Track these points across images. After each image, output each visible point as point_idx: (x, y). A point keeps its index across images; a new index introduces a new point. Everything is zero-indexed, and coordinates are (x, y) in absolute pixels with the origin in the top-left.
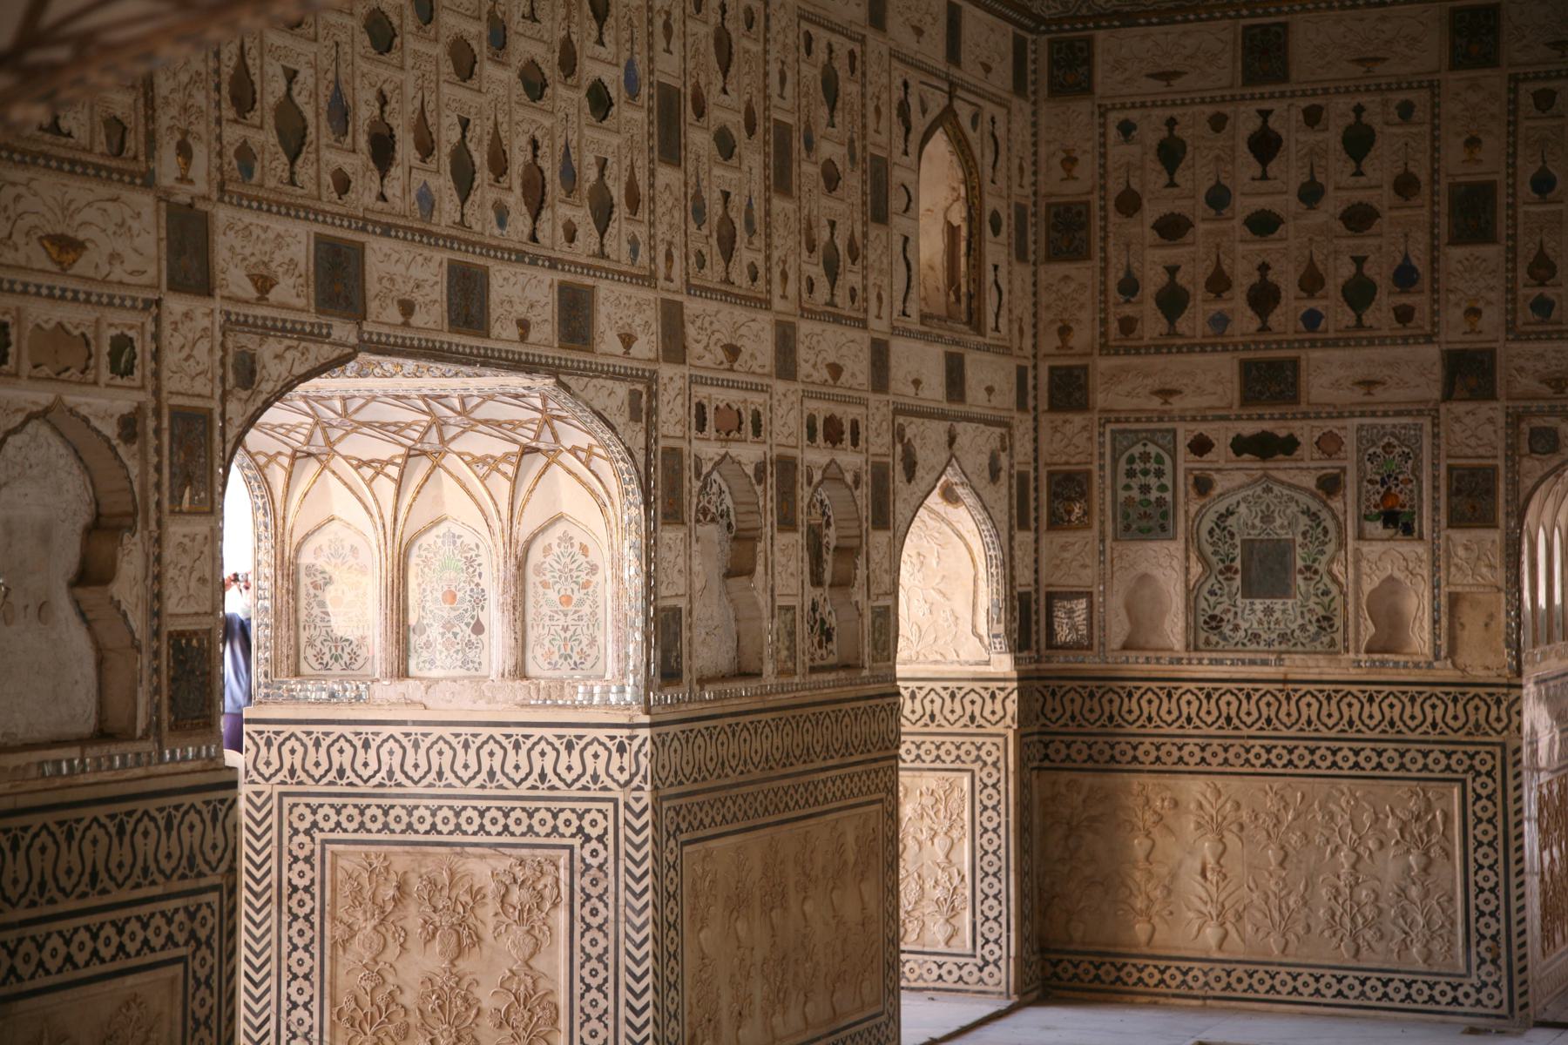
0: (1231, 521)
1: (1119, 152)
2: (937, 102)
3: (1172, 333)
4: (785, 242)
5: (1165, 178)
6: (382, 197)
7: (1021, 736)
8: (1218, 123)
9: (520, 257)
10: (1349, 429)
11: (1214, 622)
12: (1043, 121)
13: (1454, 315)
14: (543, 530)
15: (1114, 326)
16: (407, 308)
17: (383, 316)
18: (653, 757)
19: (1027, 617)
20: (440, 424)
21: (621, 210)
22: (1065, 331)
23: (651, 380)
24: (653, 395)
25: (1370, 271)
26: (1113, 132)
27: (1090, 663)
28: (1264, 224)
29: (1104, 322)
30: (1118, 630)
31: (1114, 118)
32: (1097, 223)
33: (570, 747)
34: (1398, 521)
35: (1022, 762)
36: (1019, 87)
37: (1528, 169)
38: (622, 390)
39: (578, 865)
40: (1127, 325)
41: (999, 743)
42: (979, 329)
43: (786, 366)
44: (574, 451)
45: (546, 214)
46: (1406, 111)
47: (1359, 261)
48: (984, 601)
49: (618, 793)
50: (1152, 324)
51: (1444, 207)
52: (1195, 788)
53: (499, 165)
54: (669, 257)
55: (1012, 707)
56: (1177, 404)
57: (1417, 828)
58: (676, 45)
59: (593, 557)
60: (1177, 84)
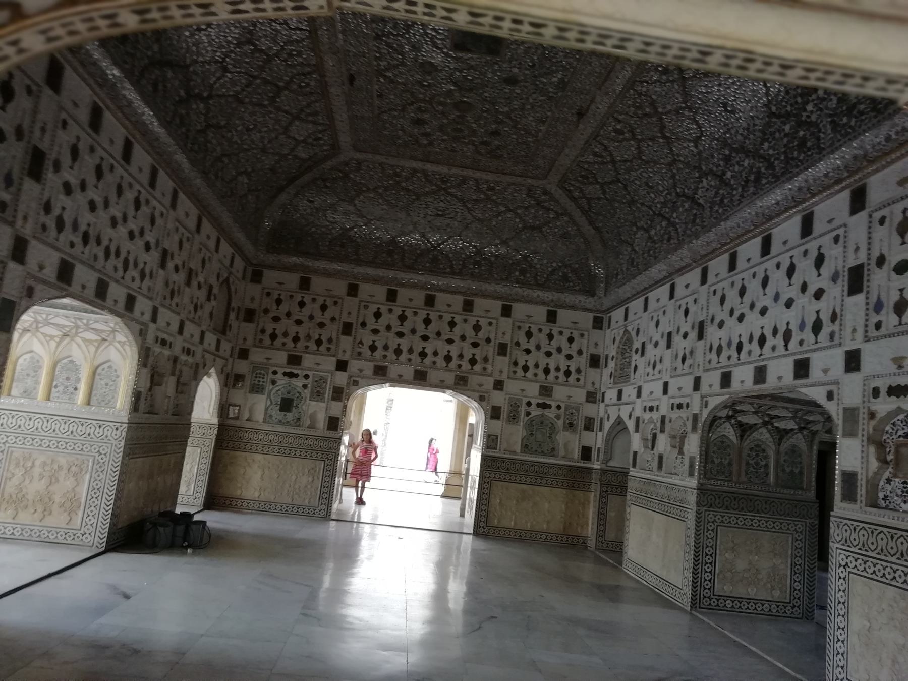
4: (186, 300)
6: (83, 253)
8: (291, 296)
9: (117, 282)
13: (340, 351)
16: (84, 287)
19: (223, 409)
20: (77, 327)
22: (245, 339)
25: (322, 338)
27: (238, 423)
30: (246, 416)
36: (244, 278)
37: (361, 320)
39: (96, 462)
40: (261, 341)
43: (181, 331)
44: (119, 342)
45: (127, 272)
46: (336, 303)
47: (320, 335)
49: (114, 443)
50: (267, 341)
51: (341, 326)
52: (259, 457)
53: (118, 254)
56: (271, 361)
57: (312, 471)
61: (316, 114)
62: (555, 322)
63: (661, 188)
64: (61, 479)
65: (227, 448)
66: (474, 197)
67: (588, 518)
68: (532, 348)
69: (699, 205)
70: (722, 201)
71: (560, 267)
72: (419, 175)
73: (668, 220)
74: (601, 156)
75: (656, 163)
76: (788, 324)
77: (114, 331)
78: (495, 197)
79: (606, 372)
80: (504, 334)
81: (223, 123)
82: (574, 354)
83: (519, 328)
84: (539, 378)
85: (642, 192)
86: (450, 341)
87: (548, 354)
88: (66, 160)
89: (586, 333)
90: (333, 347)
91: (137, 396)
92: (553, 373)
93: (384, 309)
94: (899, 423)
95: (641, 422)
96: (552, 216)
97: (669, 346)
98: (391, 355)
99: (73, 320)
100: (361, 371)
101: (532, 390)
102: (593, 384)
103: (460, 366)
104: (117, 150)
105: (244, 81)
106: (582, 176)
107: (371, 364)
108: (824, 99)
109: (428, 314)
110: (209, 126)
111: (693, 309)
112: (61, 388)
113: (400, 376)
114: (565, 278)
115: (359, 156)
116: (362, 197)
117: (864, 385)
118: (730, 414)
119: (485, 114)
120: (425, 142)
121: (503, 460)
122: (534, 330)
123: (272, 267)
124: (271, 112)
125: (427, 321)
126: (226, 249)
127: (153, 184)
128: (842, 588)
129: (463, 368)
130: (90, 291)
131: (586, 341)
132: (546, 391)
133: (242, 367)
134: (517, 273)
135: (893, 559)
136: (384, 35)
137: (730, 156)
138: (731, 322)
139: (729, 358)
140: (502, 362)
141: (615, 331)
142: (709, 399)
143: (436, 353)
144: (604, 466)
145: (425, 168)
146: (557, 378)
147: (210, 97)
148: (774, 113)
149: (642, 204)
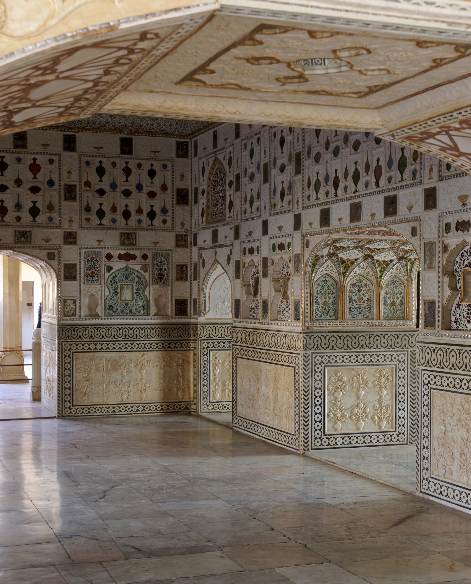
5: (99, 179)
62: (130, 152)
67: (189, 381)
68: (107, 188)
76: (378, 160)
79: (197, 210)
80: (69, 172)
83: (88, 163)
84: (117, 224)
89: (169, 164)
92: (134, 217)
94: (465, 254)
95: (241, 266)
97: (266, 180)
102: (183, 224)
103: (19, 219)
117: (439, 221)
121: (85, 327)
122: (106, 165)
128: (426, 403)
129: (23, 221)
131: (170, 174)
135: (460, 371)
138: (327, 156)
139: (327, 194)
140: (71, 210)
141: (204, 159)
142: (310, 238)
146: (140, 221)
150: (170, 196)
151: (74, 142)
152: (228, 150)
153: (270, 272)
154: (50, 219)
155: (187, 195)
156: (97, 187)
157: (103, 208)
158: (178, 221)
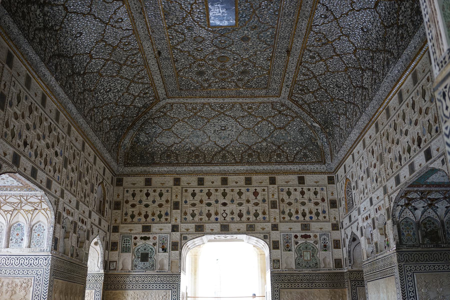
0: (140, 250)
1: (126, 194)
2: (101, 180)
3: (132, 221)
4: (79, 189)
7: (104, 283)
8: (141, 191)
10: (157, 236)
11: (136, 266)
12: (115, 189)
14: (36, 223)
15: (123, 220)
17: (21, 169)
18: (51, 261)
19: (107, 264)
20: (21, 202)
21: (57, 171)
22: (116, 220)
23: (58, 199)
24: (58, 202)
25: (162, 213)
26: (125, 191)
27: (116, 272)
28: (147, 206)
29: (122, 219)
30: (121, 267)
31: (126, 189)
32: (122, 205)
33: (36, 259)
34: (164, 250)
35: (104, 288)
36: (112, 183)
37: (184, 200)
38: (54, 199)
39: (36, 279)
40: (125, 220)
41: (100, 285)
42: (104, 216)
43: (77, 208)
44: (44, 209)
45: (47, 166)
46: (168, 191)
47: (160, 212)
48: (100, 261)
49: (44, 267)
50: (129, 220)
51: (172, 205)
53: (41, 156)
54: (63, 182)
55: (103, 278)
56: (132, 232)
57: (165, 297)
58: (68, 151)
59: (44, 228)
60: (135, 185)
61: (143, 78)
62: (304, 183)
63: (345, 86)
64: (17, 292)
65: (111, 289)
66: (242, 115)
68: (292, 201)
69: (366, 89)
70: (375, 82)
71: (301, 150)
72: (207, 106)
73: (354, 104)
74: (307, 75)
75: (338, 72)
77: (41, 202)
78: (253, 113)
79: (341, 209)
80: (273, 195)
81: (92, 89)
82: (320, 201)
84: (300, 219)
85: (336, 92)
86: (240, 204)
87: (303, 204)
88: (15, 102)
89: (325, 188)
90: (169, 217)
91: (55, 241)
92: (308, 216)
93: (197, 190)
96: (290, 119)
98: (205, 218)
99: (19, 198)
100: (187, 230)
101: (297, 227)
102: (335, 218)
103: (248, 219)
104: (39, 99)
105: (101, 63)
106: (301, 90)
107: (193, 225)
108: (405, 11)
109: (224, 190)
110: (85, 90)
111: (375, 149)
112: (14, 240)
113: (212, 230)
114: (305, 156)
115: (170, 101)
116: (176, 126)
118: (406, 202)
119: (236, 62)
120: (207, 85)
123: (128, 175)
124: (118, 80)
125: (224, 194)
126: (100, 164)
127: (57, 119)
129: (251, 220)
130: (28, 172)
131: (325, 193)
132: (305, 227)
133: (116, 237)
134: (275, 157)
136: (172, 25)
137: (373, 56)
142: (392, 196)
143: (232, 213)
144: (350, 268)
145: (209, 101)
146: (311, 218)
147: (85, 73)
148: (386, 26)
149: (338, 99)
150: (327, 204)
151: (275, 180)
152: (351, 171)
153: (376, 225)
154: (264, 218)
155: (336, 203)
156: (288, 201)
157: (291, 211)
158: (332, 217)
